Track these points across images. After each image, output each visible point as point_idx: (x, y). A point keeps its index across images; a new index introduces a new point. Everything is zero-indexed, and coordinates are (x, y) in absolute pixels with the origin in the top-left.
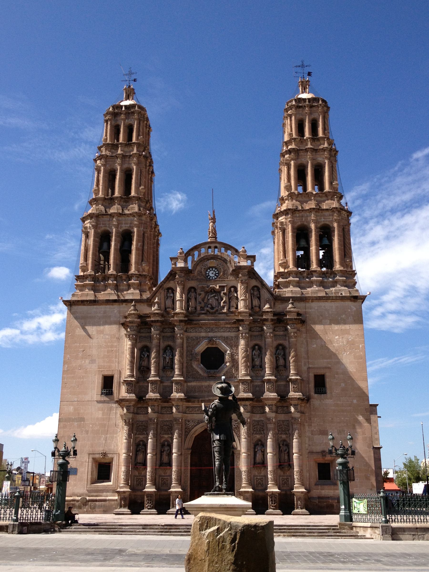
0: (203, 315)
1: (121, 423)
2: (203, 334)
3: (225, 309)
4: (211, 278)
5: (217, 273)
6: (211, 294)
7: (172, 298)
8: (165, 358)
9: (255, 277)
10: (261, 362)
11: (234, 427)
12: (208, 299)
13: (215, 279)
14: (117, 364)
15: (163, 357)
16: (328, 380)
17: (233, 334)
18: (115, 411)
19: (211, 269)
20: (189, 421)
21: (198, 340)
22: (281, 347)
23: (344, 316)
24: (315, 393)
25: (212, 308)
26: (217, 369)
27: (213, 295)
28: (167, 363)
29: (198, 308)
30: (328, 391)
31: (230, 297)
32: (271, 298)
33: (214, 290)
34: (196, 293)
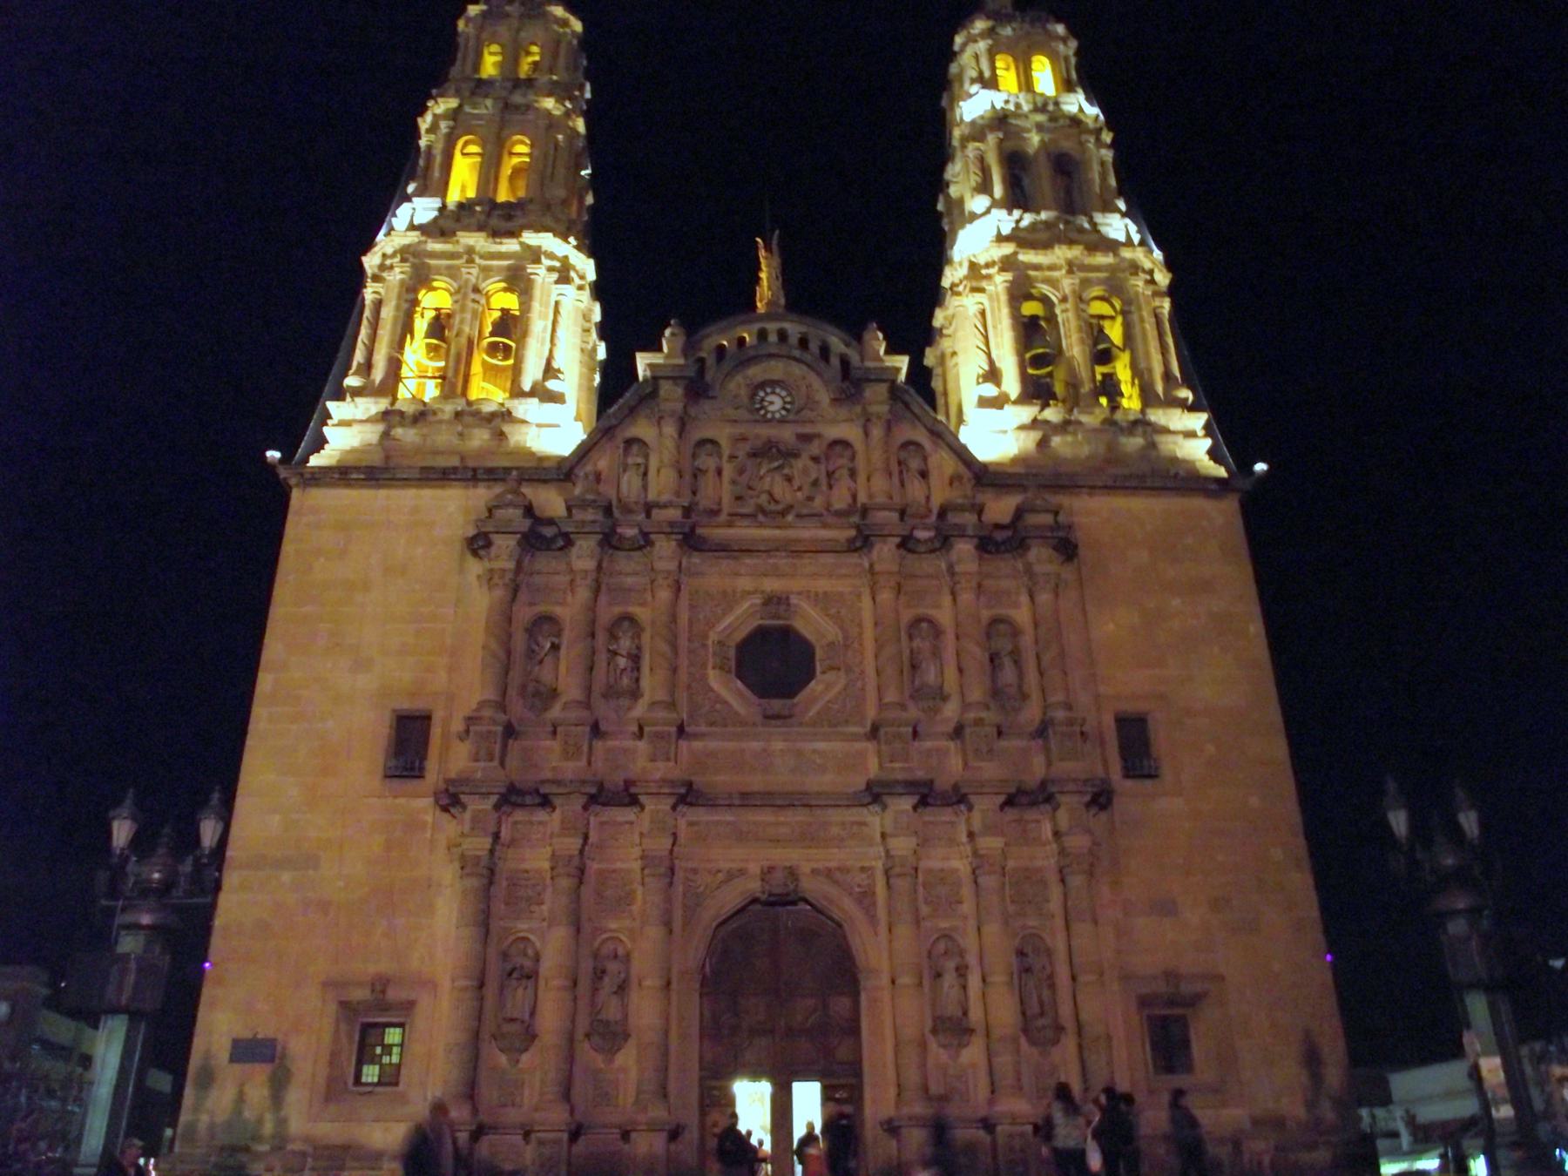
0: (746, 522)
1: (447, 874)
2: (745, 583)
3: (818, 502)
4: (769, 416)
5: (789, 403)
6: (770, 463)
7: (642, 469)
8: (615, 653)
9: (908, 415)
10: (942, 673)
11: (857, 890)
12: (761, 478)
13: (783, 416)
14: (443, 675)
15: (609, 651)
16: (1161, 737)
17: (842, 586)
18: (428, 835)
19: (769, 390)
20: (695, 871)
21: (729, 599)
22: (1002, 627)
23: (1189, 541)
24: (1130, 772)
25: (777, 502)
26: (791, 694)
27: (776, 464)
28: (618, 672)
29: (727, 499)
30: (1166, 771)
31: (831, 468)
32: (967, 474)
33: (779, 451)
34: (720, 457)
